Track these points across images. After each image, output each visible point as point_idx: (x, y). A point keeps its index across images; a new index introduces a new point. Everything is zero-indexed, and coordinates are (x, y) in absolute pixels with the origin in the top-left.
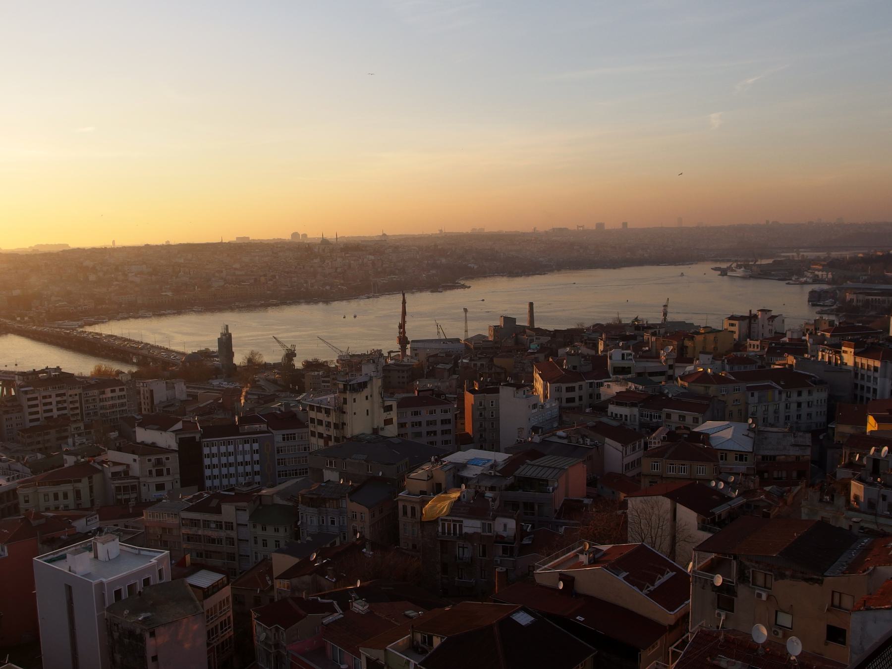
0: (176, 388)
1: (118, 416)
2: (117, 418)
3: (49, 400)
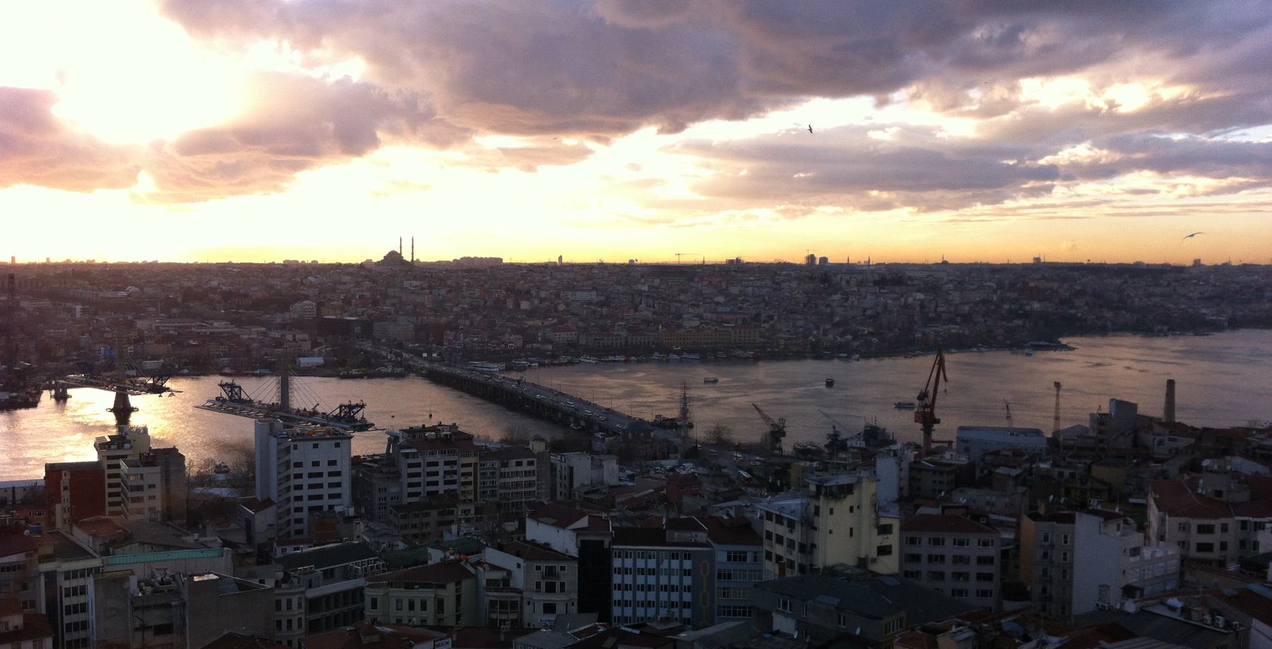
1: (523, 500)
3: (433, 469)
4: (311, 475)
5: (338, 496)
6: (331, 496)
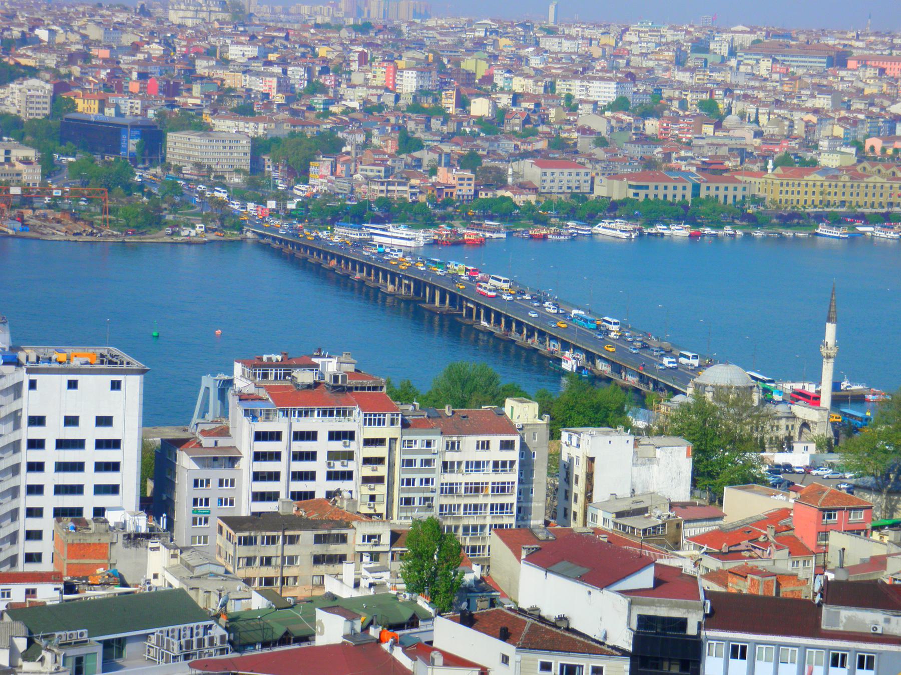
0: (662, 462)
1: (489, 521)
2: (483, 527)
4: (61, 444)
5: (114, 489)
6: (100, 490)
